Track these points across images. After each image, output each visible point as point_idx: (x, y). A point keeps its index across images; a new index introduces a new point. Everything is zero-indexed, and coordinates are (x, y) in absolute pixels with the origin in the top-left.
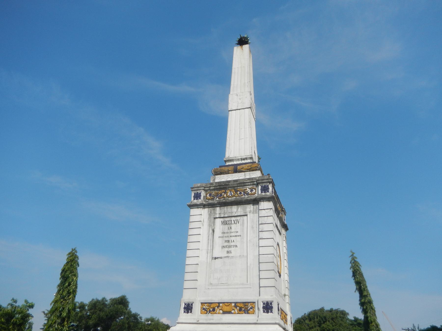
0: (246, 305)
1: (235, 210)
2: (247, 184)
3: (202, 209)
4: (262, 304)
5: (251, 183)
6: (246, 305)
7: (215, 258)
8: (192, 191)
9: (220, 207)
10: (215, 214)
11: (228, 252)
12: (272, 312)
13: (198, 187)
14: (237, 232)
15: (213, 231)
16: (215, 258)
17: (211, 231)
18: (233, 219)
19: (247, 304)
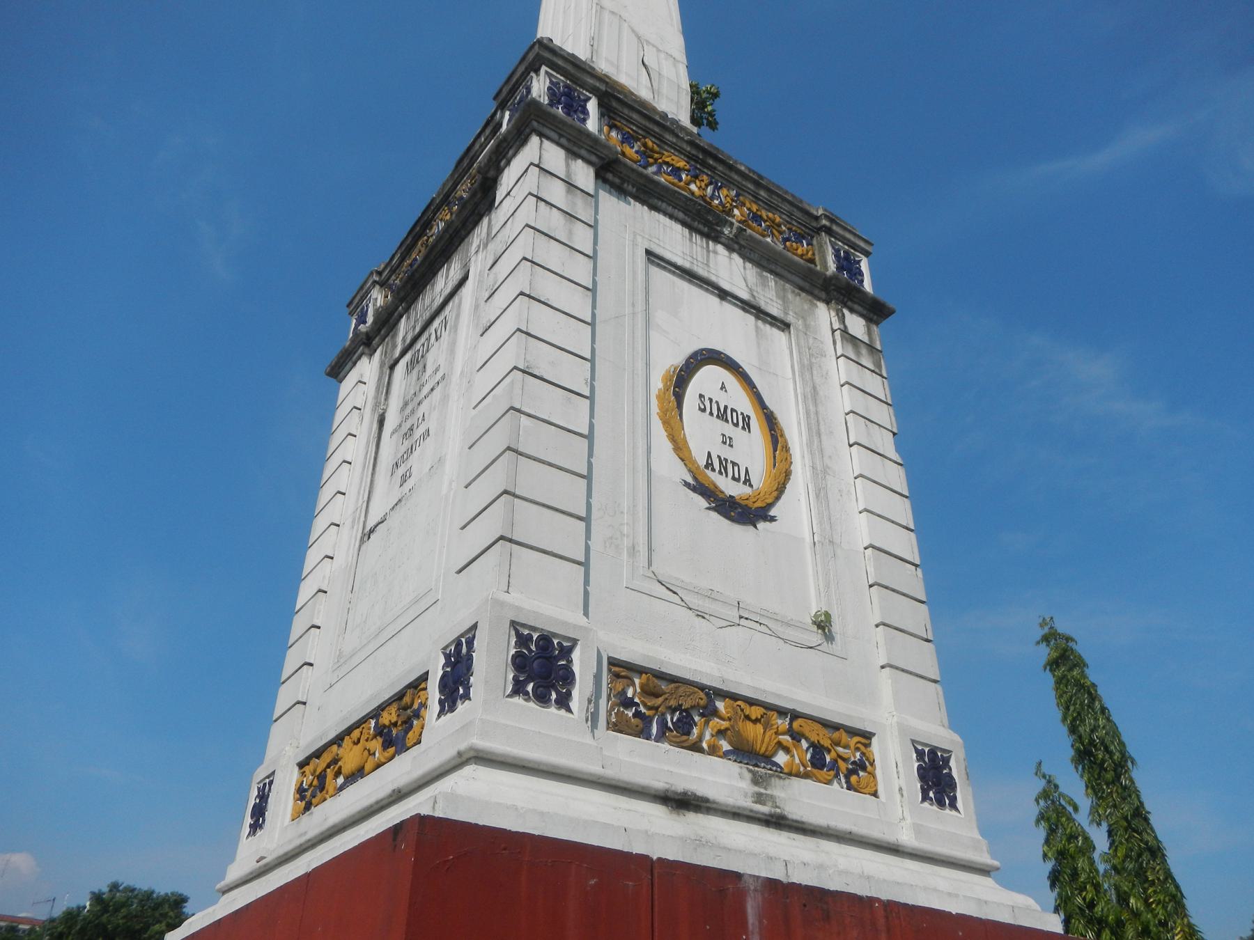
0: (405, 708)
1: (442, 284)
2: (477, 146)
3: (365, 360)
4: (442, 661)
5: (488, 132)
6: (405, 708)
7: (372, 531)
8: (351, 314)
9: (407, 310)
10: (394, 346)
11: (404, 479)
12: (466, 696)
13: (362, 288)
14: (437, 370)
15: (381, 422)
16: (372, 531)
17: (375, 426)
18: (436, 323)
19: (407, 699)
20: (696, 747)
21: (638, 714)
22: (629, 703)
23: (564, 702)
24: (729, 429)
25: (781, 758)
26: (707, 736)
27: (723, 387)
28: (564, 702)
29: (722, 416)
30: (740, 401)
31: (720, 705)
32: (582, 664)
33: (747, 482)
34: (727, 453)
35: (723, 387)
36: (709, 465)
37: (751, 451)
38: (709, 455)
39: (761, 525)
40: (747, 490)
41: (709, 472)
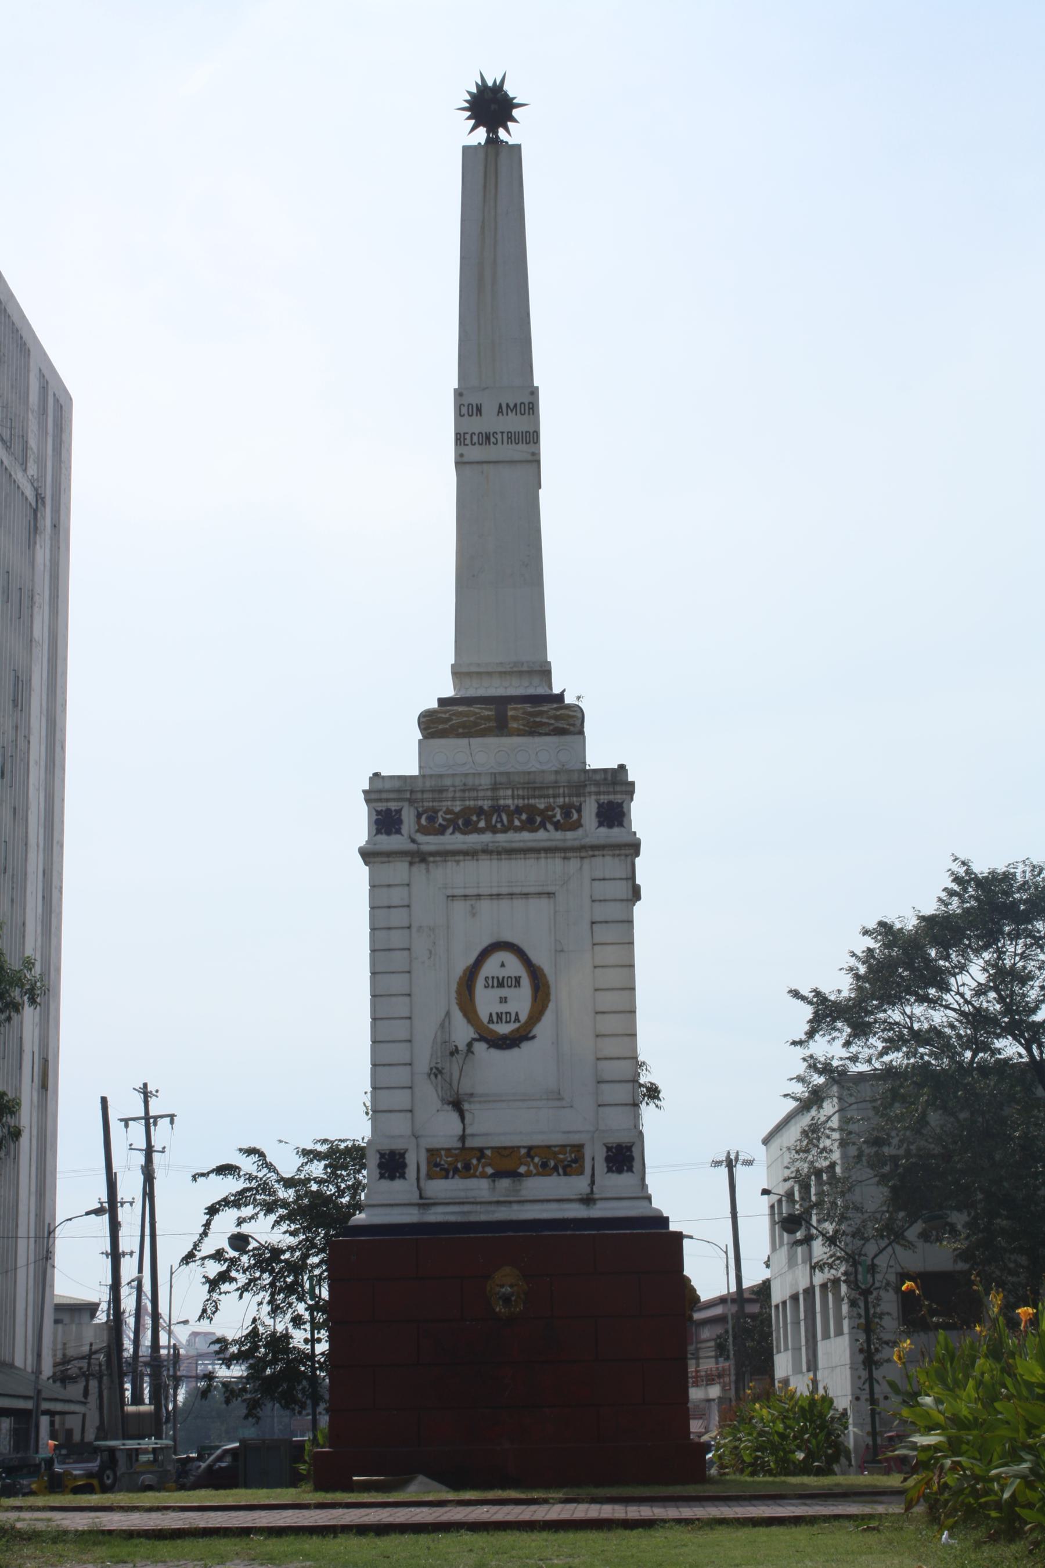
20: (474, 1176)
21: (441, 1169)
22: (436, 1165)
23: (403, 1176)
24: (504, 992)
25: (522, 1170)
26: (480, 1169)
27: (503, 965)
28: (403, 1176)
29: (501, 985)
30: (514, 967)
31: (488, 1153)
32: (411, 1159)
33: (517, 1020)
34: (503, 1008)
35: (503, 965)
36: (491, 1021)
37: (521, 1001)
38: (491, 1015)
39: (526, 1046)
40: (513, 1026)
41: (491, 1026)
